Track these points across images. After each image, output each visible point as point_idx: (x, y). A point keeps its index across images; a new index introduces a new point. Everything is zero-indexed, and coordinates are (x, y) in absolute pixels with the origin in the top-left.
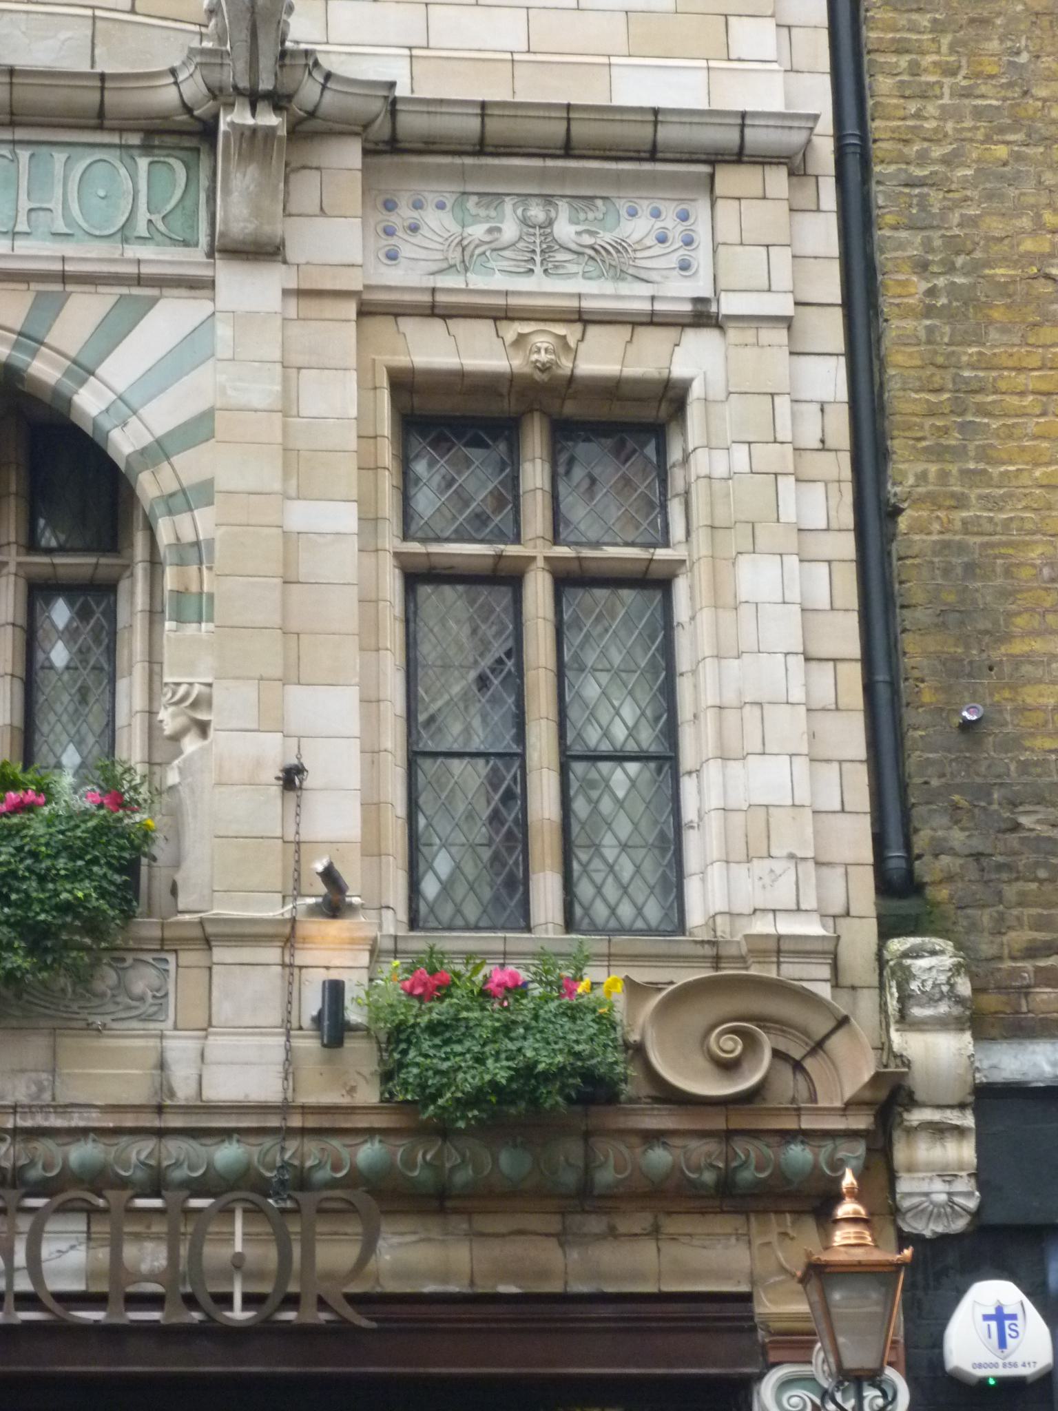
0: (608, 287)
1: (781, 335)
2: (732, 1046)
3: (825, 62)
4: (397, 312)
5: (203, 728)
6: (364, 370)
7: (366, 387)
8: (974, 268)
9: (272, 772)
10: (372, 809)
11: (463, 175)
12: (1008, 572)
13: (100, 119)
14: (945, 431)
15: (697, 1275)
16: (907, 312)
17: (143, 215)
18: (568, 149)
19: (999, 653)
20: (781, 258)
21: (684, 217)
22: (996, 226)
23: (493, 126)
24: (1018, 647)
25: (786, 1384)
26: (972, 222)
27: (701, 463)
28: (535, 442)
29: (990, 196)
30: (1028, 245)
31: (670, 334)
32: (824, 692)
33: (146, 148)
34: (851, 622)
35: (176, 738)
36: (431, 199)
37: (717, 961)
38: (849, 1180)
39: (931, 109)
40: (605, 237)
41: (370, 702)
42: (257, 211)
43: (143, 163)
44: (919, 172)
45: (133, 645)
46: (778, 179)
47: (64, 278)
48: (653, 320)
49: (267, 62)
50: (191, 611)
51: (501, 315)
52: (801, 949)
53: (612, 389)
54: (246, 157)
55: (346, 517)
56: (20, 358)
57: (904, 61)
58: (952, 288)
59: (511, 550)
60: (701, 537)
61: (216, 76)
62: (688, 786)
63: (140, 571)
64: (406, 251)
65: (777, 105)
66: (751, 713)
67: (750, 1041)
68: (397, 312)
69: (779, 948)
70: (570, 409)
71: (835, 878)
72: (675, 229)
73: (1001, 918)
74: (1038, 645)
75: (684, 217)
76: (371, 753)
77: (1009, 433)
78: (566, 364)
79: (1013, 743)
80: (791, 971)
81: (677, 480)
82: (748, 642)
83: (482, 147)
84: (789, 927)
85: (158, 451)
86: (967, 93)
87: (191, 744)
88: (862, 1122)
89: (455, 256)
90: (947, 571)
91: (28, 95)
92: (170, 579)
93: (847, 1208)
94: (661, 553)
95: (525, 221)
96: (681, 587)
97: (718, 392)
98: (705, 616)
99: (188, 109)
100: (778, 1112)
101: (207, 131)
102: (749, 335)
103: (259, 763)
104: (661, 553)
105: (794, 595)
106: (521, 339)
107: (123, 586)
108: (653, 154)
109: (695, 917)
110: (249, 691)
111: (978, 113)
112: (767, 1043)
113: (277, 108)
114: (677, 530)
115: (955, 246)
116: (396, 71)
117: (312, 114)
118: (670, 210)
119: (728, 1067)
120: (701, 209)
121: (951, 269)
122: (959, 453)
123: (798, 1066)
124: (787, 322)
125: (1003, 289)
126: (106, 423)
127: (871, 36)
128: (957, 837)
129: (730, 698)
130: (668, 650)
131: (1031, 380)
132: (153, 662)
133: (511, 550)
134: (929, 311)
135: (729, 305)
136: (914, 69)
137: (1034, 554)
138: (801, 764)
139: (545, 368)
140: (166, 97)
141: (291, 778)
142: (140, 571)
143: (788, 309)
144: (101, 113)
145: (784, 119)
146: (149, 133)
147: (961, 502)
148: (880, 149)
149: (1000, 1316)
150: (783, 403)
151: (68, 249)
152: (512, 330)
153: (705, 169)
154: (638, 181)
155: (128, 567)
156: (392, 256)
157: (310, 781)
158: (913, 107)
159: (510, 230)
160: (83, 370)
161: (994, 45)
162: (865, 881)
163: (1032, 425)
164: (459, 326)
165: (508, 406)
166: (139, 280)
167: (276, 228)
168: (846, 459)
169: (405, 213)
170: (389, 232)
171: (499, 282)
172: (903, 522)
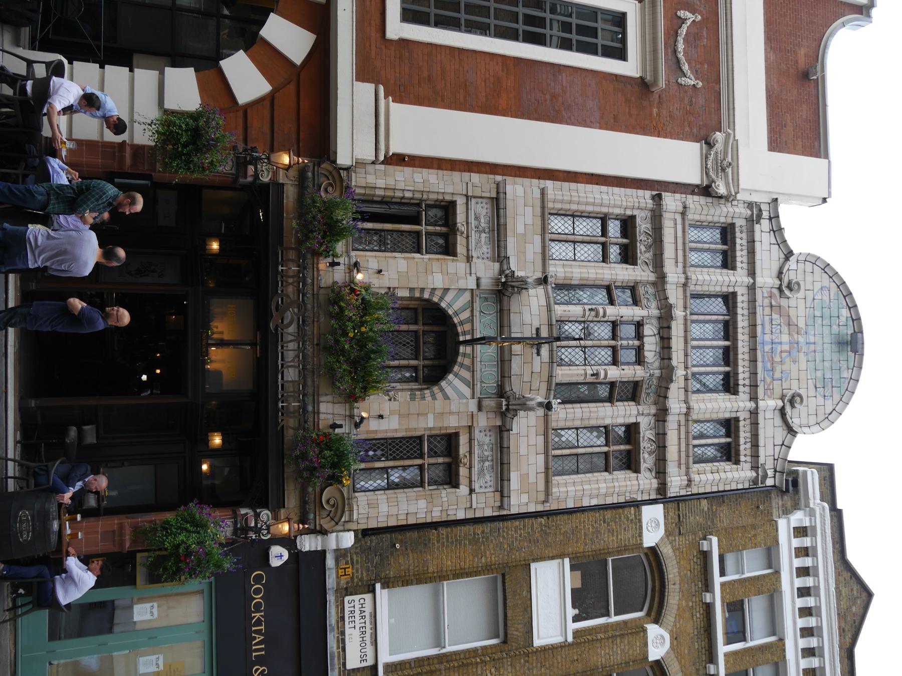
0: (476, 473)
1: (468, 506)
2: (332, 502)
3: (520, 512)
4: (470, 433)
5: (390, 400)
6: (459, 427)
7: (455, 428)
8: (483, 542)
9: (382, 413)
10: (376, 432)
11: (496, 444)
12: (425, 552)
13: (503, 377)
14: (452, 538)
15: (288, 498)
16: (474, 530)
17: (486, 385)
18: (502, 464)
19: (409, 551)
20: (483, 505)
21: (490, 486)
22: (491, 546)
23: (505, 449)
24: (410, 555)
25: (268, 515)
26: (492, 542)
27: (444, 492)
28: (447, 460)
29: (497, 544)
30: (488, 552)
31: (468, 485)
32: (401, 517)
33: (498, 385)
34: (414, 522)
35: (388, 395)
36: (492, 438)
37: (349, 499)
38: (306, 526)
39: (513, 533)
40: (486, 471)
41: (396, 431)
42: (487, 406)
43: (495, 385)
45: (406, 386)
46: (498, 504)
47: (473, 371)
48: (470, 481)
49: (514, 407)
50: (412, 396)
51: (470, 452)
52: (351, 515)
54: (497, 404)
55: (431, 425)
56: (458, 364)
57: (522, 527)
58: (479, 538)
59: (426, 456)
60: (430, 493)
61: (511, 398)
62: (382, 492)
63: (420, 387)
64: (482, 434)
65: (512, 503)
66: (396, 503)
67: (333, 506)
68: (470, 433)
69: (351, 511)
70: (453, 466)
71: (365, 521)
72: (488, 485)
73: (358, 553)
74: (411, 558)
75: (490, 486)
76: (386, 431)
77: (452, 551)
78: (462, 465)
79: (392, 554)
80: (347, 513)
81: (441, 487)
82: (409, 502)
83: (502, 447)
84: (355, 512)
86: (516, 539)
87: (387, 398)
88: (318, 528)
89: (481, 443)
90: (425, 540)
91: (506, 364)
92: (418, 393)
93: (301, 526)
94: (426, 485)
95: (488, 456)
96: (421, 489)
97: (457, 494)
98: (415, 494)
99: (505, 393)
100: (319, 512)
101: (502, 397)
102: (468, 500)
103: (383, 410)
104: (426, 485)
105: (419, 511)
106: (466, 456)
108: (502, 480)
109: (357, 494)
110: (397, 408)
111: (513, 542)
112: (333, 510)
113: (506, 409)
114: (431, 488)
115: (487, 539)
116: (515, 431)
117: (505, 416)
118: (491, 483)
119: (328, 502)
120: (492, 489)
121: (483, 538)
122: (448, 541)
123: (328, 515)
124: (471, 507)
125: (480, 548)
126: (447, 380)
127: (526, 520)
128: (374, 544)
129: (399, 499)
130: (409, 487)
132: (402, 390)
133: (426, 456)
134: (474, 534)
135: (474, 496)
137: (429, 557)
138: (387, 513)
139: (461, 461)
140: (507, 388)
141: (381, 417)
142: (420, 387)
143: (474, 506)
144: (504, 377)
145: (509, 504)
146: (501, 386)
147: (438, 542)
148: (505, 524)
149: (281, 556)
150: (456, 507)
154: (497, 477)
155: (420, 384)
156: (480, 431)
157: (380, 420)
159: (486, 453)
160: (456, 375)
161: (526, 544)
162: (365, 527)
163: (454, 555)
164: (468, 445)
166: (473, 385)
167: (484, 409)
168: (446, 519)
169: (489, 434)
170: (485, 431)
171: (476, 452)
172: (434, 531)
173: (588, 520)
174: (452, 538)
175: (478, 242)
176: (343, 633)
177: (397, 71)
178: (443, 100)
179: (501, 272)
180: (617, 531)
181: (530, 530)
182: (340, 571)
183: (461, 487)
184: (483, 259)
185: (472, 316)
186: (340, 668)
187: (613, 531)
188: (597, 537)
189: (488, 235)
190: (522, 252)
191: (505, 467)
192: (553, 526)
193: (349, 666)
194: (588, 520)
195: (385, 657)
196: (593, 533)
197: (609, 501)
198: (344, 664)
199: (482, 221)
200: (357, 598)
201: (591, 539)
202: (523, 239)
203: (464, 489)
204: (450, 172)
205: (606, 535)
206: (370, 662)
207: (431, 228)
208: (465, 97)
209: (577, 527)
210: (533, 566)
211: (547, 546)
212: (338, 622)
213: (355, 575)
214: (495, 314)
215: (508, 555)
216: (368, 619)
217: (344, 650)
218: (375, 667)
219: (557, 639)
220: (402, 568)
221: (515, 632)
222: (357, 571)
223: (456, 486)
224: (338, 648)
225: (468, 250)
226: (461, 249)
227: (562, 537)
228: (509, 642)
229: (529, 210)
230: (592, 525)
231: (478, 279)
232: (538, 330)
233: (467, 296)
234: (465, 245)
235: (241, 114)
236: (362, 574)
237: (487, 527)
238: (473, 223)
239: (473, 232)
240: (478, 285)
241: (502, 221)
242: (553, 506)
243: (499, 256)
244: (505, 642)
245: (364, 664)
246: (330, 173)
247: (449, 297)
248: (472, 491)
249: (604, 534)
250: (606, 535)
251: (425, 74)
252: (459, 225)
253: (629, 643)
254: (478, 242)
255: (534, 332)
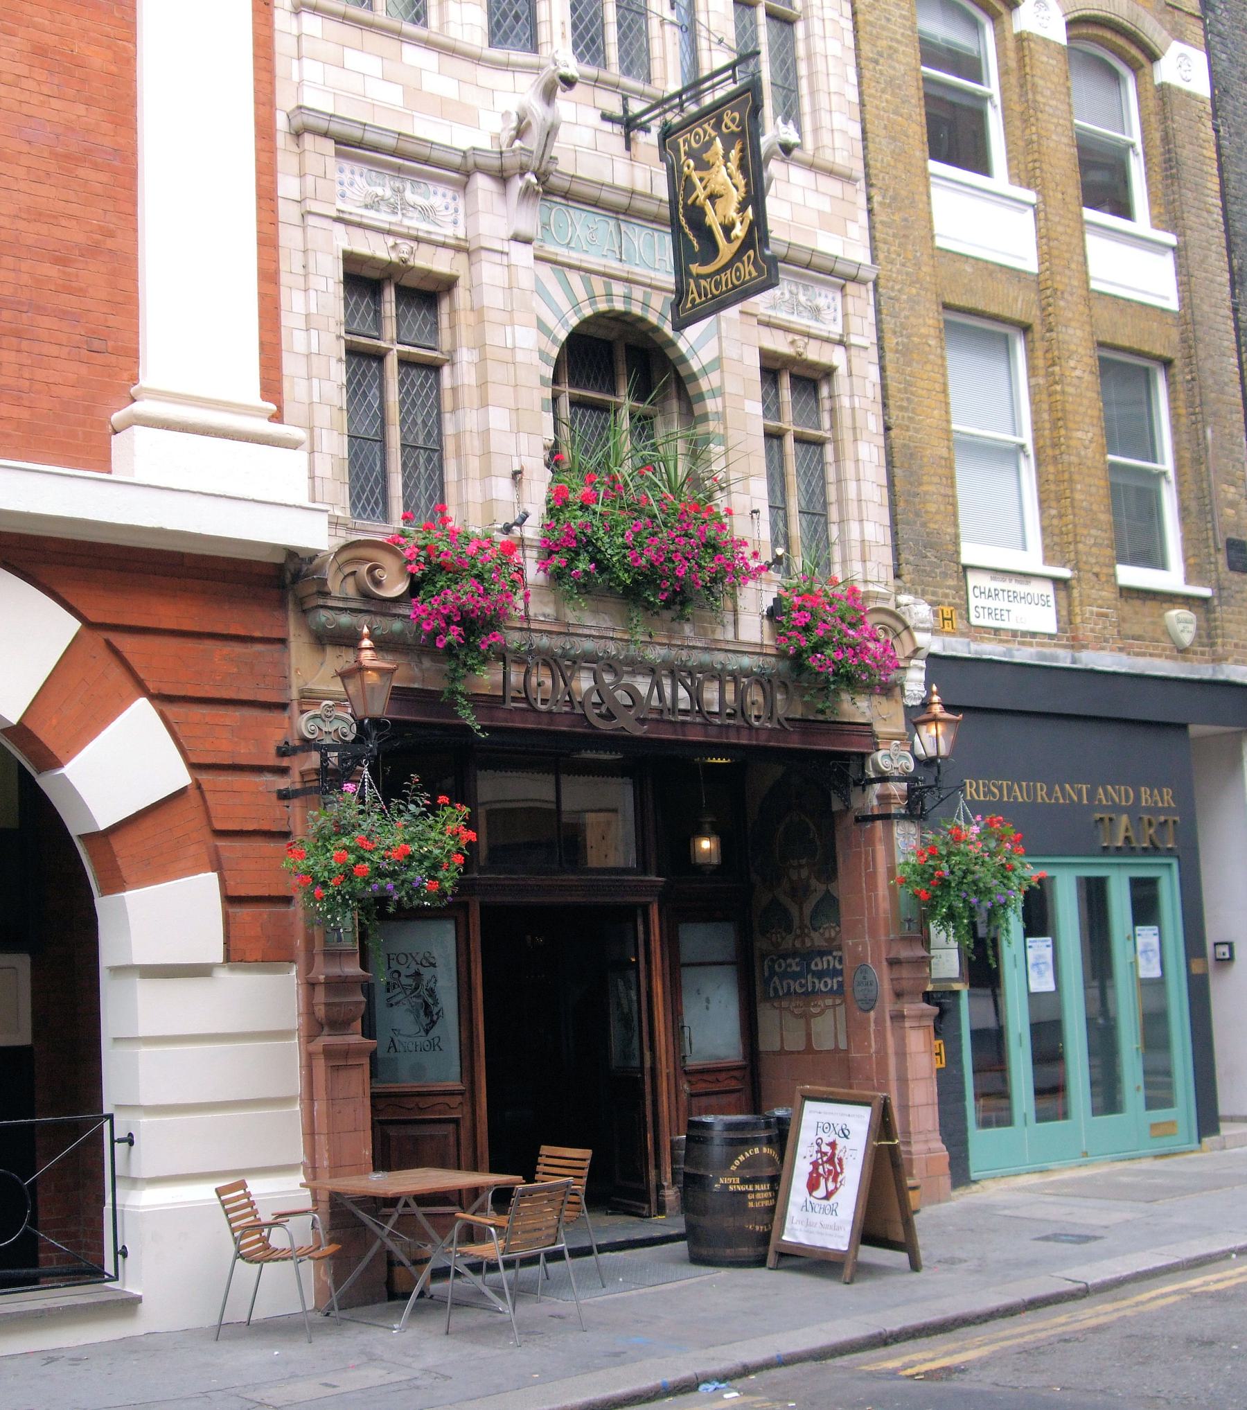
8: (908, 337)
14: (902, 399)
18: (808, 266)
19: (919, 490)
22: (913, 320)
24: (925, 488)
25: (884, 756)
27: (845, 402)
44: (893, 294)
48: (827, 340)
51: (787, 330)
53: (813, 366)
58: (904, 345)
75: (834, 299)
85: (705, 370)
86: (903, 265)
95: (791, 292)
96: (829, 449)
107: (658, 421)
111: (907, 274)
114: (826, 422)
120: (838, 296)
126: (688, 356)
128: (912, 558)
131: (925, 384)
135: (854, 340)
136: (889, 252)
137: (928, 452)
147: (908, 430)
151: (652, 274)
152: (790, 337)
153: (842, 282)
158: (889, 267)
159: (787, 296)
165: (778, 365)
173: (875, 97)
174: (902, 399)
175: (425, 212)
176: (1014, 633)
177: (54, 350)
178: (110, 234)
179: (502, 177)
180: (892, 39)
181: (891, 232)
182: (947, 629)
183: (835, 363)
184: (456, 211)
185: (579, 269)
186: (1056, 645)
187: (890, 47)
188: (899, 87)
189: (408, 186)
190: (444, 108)
191: (816, 261)
192: (884, 179)
193: (1052, 628)
194: (875, 97)
195: (1032, 559)
196: (893, 94)
197: (849, 40)
198: (1051, 636)
199: (379, 191)
200: (973, 602)
201: (903, 102)
202: (413, 92)
203: (837, 357)
204: (281, 251)
205: (897, 66)
206: (1048, 589)
207: (390, 328)
208: (96, 167)
209: (885, 127)
210: (939, 242)
211: (913, 204)
212: (1001, 641)
213: (951, 600)
214: (572, 211)
215: (927, 290)
216: (999, 585)
217: (1034, 635)
218: (1058, 582)
219: (1026, 223)
220: (942, 508)
221: (1019, 305)
222: (946, 596)
223: (828, 373)
224: (1031, 644)
225: (444, 245)
226: (441, 263)
227: (900, 166)
228: (1030, 321)
229: (353, 59)
230: (883, 91)
231: (516, 238)
232: (606, 117)
233: (545, 270)
234: (431, 249)
235: (204, 777)
236: (949, 587)
237: (888, 324)
238: (382, 218)
239: (407, 222)
240: (528, 241)
241: (390, 141)
242: (858, 169)
243: (457, 170)
244: (1026, 329)
245: (1052, 599)
246: (339, 569)
247: (551, 321)
248: (841, 343)
249: (894, 69)
250: (897, 66)
251: (52, 271)
252: (394, 257)
253: (1042, 78)
254: (425, 212)
255: (608, 126)
